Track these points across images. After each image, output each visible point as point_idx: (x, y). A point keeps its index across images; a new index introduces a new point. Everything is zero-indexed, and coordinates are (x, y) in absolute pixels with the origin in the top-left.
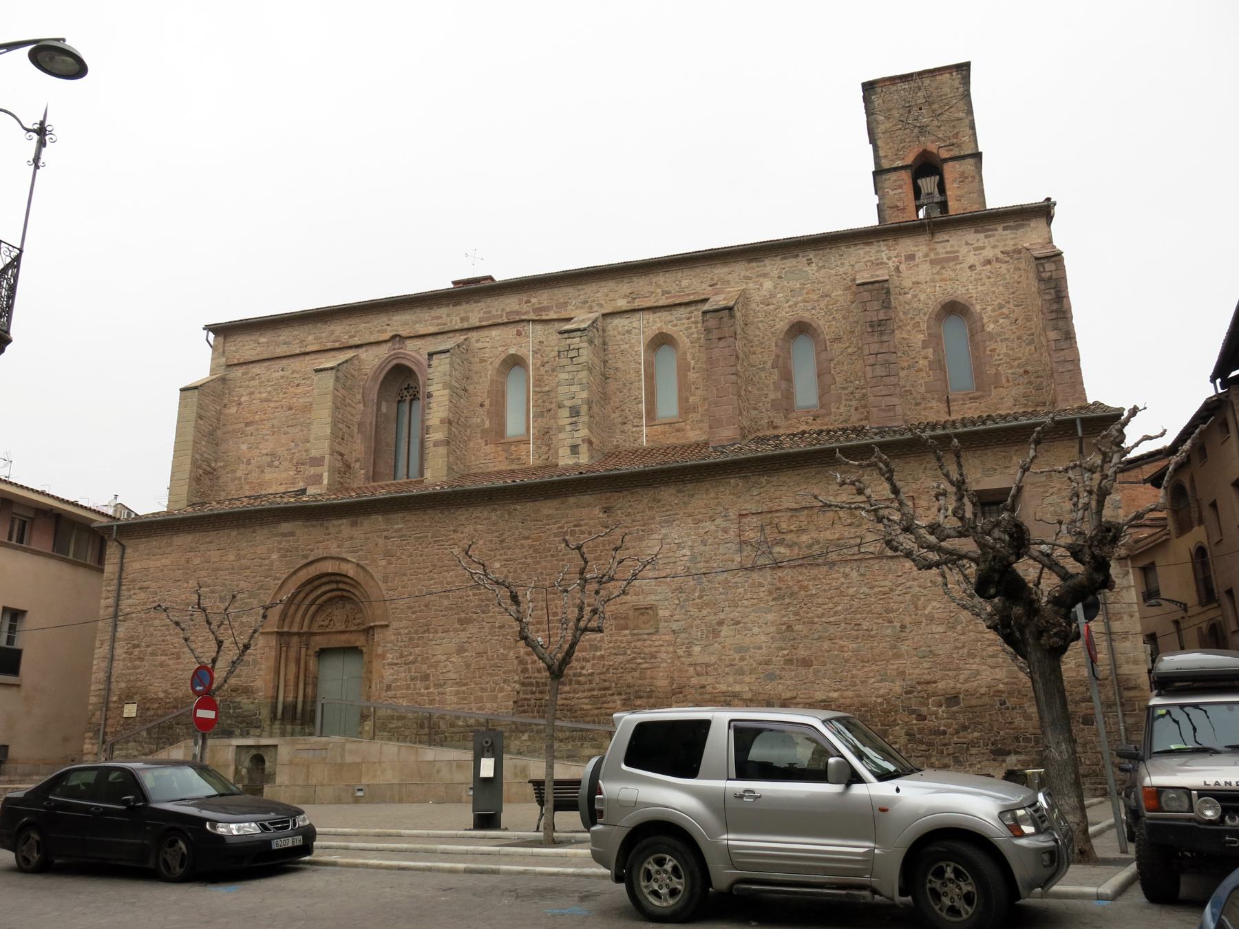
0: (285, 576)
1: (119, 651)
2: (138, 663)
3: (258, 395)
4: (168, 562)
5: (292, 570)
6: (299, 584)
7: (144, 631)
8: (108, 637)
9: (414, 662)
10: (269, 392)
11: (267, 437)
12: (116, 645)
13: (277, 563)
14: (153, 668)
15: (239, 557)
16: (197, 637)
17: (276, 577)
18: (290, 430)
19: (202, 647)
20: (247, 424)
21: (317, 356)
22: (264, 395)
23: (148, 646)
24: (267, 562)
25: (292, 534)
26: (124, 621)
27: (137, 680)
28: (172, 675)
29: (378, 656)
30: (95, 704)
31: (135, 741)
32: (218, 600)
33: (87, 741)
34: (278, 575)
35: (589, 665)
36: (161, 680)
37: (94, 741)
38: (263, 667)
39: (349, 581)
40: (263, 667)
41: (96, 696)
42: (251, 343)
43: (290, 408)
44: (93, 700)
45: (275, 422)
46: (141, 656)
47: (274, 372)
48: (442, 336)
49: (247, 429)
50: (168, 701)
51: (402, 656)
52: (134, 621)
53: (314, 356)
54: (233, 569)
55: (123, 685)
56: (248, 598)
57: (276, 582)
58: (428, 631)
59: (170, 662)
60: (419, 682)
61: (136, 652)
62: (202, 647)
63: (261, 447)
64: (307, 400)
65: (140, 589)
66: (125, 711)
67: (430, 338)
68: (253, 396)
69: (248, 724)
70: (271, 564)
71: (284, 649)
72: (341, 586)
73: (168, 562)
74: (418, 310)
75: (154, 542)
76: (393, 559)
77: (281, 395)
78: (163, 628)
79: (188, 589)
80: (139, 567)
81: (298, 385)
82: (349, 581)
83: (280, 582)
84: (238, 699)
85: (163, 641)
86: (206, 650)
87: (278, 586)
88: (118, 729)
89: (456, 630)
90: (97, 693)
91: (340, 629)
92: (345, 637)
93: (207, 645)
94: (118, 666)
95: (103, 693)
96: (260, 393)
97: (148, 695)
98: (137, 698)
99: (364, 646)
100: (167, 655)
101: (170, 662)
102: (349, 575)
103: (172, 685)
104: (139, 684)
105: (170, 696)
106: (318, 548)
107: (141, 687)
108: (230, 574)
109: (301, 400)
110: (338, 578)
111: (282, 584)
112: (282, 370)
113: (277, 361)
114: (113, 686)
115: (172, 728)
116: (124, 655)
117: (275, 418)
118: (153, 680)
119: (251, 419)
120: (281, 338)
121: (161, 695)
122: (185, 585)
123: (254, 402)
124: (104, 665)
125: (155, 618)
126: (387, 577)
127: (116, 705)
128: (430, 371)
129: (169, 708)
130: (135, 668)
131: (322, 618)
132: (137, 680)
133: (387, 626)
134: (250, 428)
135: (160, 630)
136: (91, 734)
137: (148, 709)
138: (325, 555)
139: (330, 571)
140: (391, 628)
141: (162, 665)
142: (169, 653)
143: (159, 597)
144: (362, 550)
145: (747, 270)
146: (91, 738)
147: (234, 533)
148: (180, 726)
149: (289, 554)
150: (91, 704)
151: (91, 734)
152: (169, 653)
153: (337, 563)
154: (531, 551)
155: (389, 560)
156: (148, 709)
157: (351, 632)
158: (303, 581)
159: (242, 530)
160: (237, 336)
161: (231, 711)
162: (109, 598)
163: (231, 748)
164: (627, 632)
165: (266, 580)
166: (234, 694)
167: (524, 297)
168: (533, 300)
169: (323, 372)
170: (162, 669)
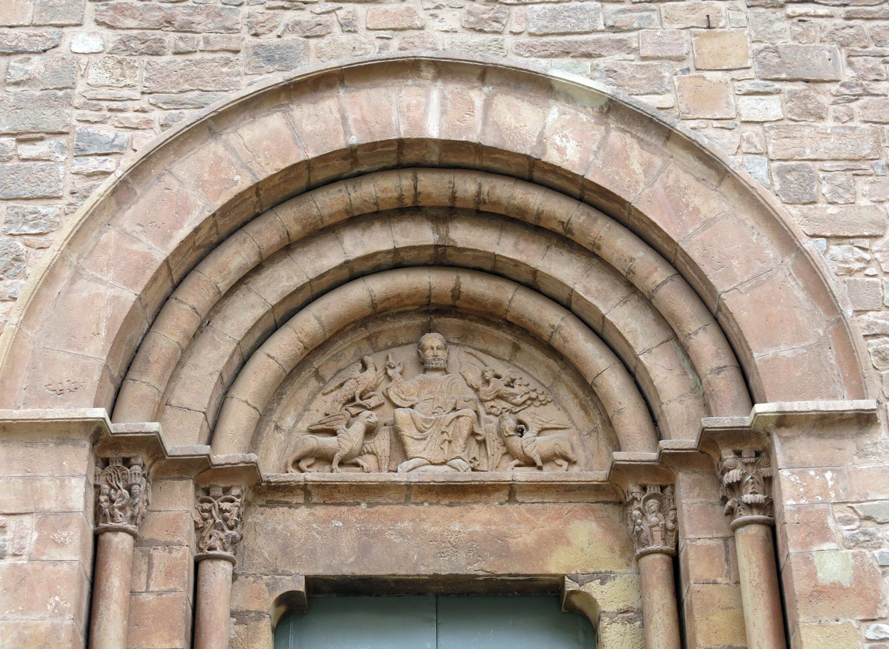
0: (147, 141)
5: (190, 116)
6: (244, 182)
13: (94, 75)
17: (92, 139)
24: (36, 64)
34: (106, 132)
57: (93, 164)
71: (120, 543)
76: (824, 96)
83: (119, 166)
87: (105, 185)
91: (439, 474)
99: (604, 578)
102: (553, 157)
106: (348, 27)
111: (138, 171)
126: (810, 179)
131: (315, 417)
138: (394, 50)
139: (433, 130)
144: (621, 45)
149: (171, 38)
153: (477, 96)
155: (793, 95)
157: (512, 491)
158: (267, 168)
165: (27, 150)
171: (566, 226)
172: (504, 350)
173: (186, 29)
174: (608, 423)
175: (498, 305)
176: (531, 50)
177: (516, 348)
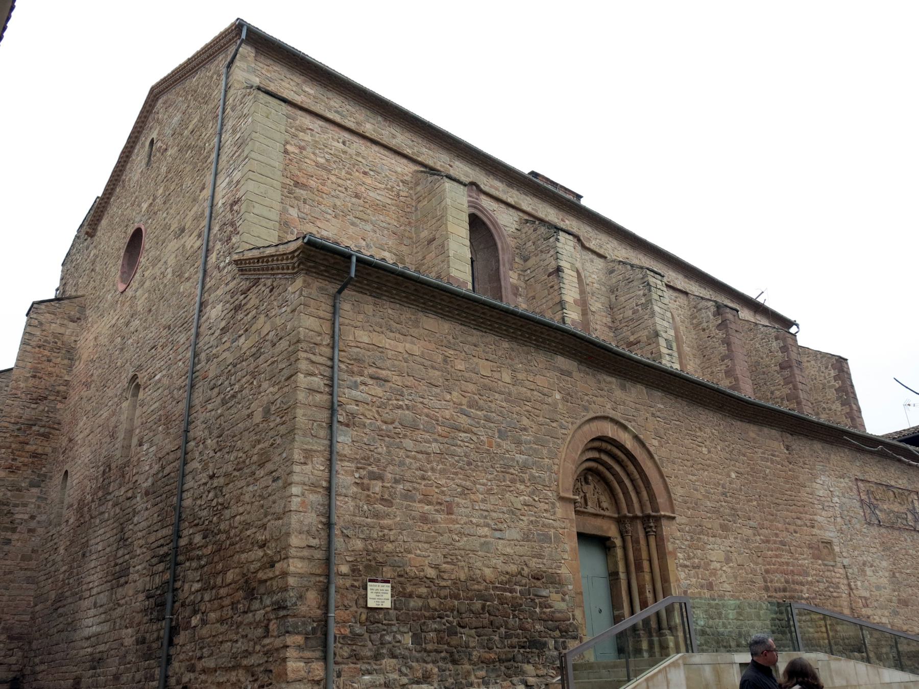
1: (345, 479)
2: (379, 507)
3: (312, 156)
4: (416, 349)
7: (389, 452)
8: (320, 445)
9: (698, 567)
10: (327, 160)
11: (329, 217)
12: (338, 466)
14: (411, 522)
15: (515, 382)
16: (474, 483)
18: (357, 221)
19: (483, 501)
20: (297, 184)
21: (386, 153)
22: (322, 161)
23: (397, 481)
25: (569, 374)
26: (347, 425)
27: (383, 539)
28: (445, 538)
29: (670, 553)
30: (301, 576)
31: (394, 656)
32: (497, 435)
33: (291, 653)
35: (805, 589)
36: (426, 546)
37: (308, 654)
38: (568, 548)
39: (619, 453)
40: (568, 548)
41: (302, 558)
42: (292, 83)
43: (357, 196)
44: (296, 566)
45: (338, 203)
46: (386, 497)
47: (334, 139)
48: (514, 211)
49: (297, 190)
50: (443, 583)
51: (689, 558)
52: (367, 431)
53: (382, 151)
54: (510, 394)
55: (359, 544)
56: (534, 443)
58: (701, 533)
59: (439, 517)
60: (706, 591)
61: (377, 486)
62: (483, 501)
63: (318, 223)
64: (378, 198)
65: (372, 377)
66: (370, 595)
67: (503, 206)
68: (304, 152)
69: (561, 631)
70: (555, 405)
72: (605, 458)
73: (416, 349)
74: (477, 169)
75: (390, 310)
77: (343, 173)
78: (420, 456)
79: (451, 404)
80: (366, 339)
81: (365, 173)
82: (619, 453)
84: (545, 593)
85: (423, 478)
86: (489, 507)
88: (358, 630)
89: (720, 537)
90: (306, 553)
92: (598, 522)
93: (493, 499)
94: (344, 507)
95: (319, 554)
96: (314, 153)
97: (408, 569)
98: (388, 572)
99: (616, 538)
100: (429, 503)
101: (439, 517)
103: (445, 557)
104: (389, 547)
105: (446, 576)
107: (388, 554)
108: (506, 400)
109: (371, 194)
110: (609, 447)
112: (344, 143)
113: (336, 129)
114: (339, 543)
115: (456, 634)
116: (355, 489)
117: (337, 197)
118: (413, 545)
119: (304, 181)
120: (332, 103)
121: (432, 573)
122: (448, 397)
123: (306, 160)
124: (316, 498)
125: (405, 436)
127: (348, 583)
128: (558, 244)
129: (445, 598)
130: (377, 515)
132: (383, 539)
133: (674, 518)
134: (302, 192)
135: (415, 458)
136: (299, 639)
137: (410, 596)
140: (674, 522)
141: (424, 519)
142: (434, 501)
143: (407, 402)
145: (685, 282)
146: (299, 647)
147: (506, 345)
148: (466, 630)
150: (295, 575)
151: (299, 639)
152: (434, 501)
154: (749, 469)
156: (410, 596)
159: (515, 345)
160: (272, 62)
161: (538, 610)
162: (315, 375)
163: (734, 666)
164: (820, 562)
166: (538, 583)
167: (561, 215)
168: (567, 222)
169: (456, 184)
170: (426, 528)
171: (623, 461)
172: (596, 481)
173: (571, 396)
174: (616, 503)
175: (602, 472)
176: (622, 418)
177: (599, 481)
